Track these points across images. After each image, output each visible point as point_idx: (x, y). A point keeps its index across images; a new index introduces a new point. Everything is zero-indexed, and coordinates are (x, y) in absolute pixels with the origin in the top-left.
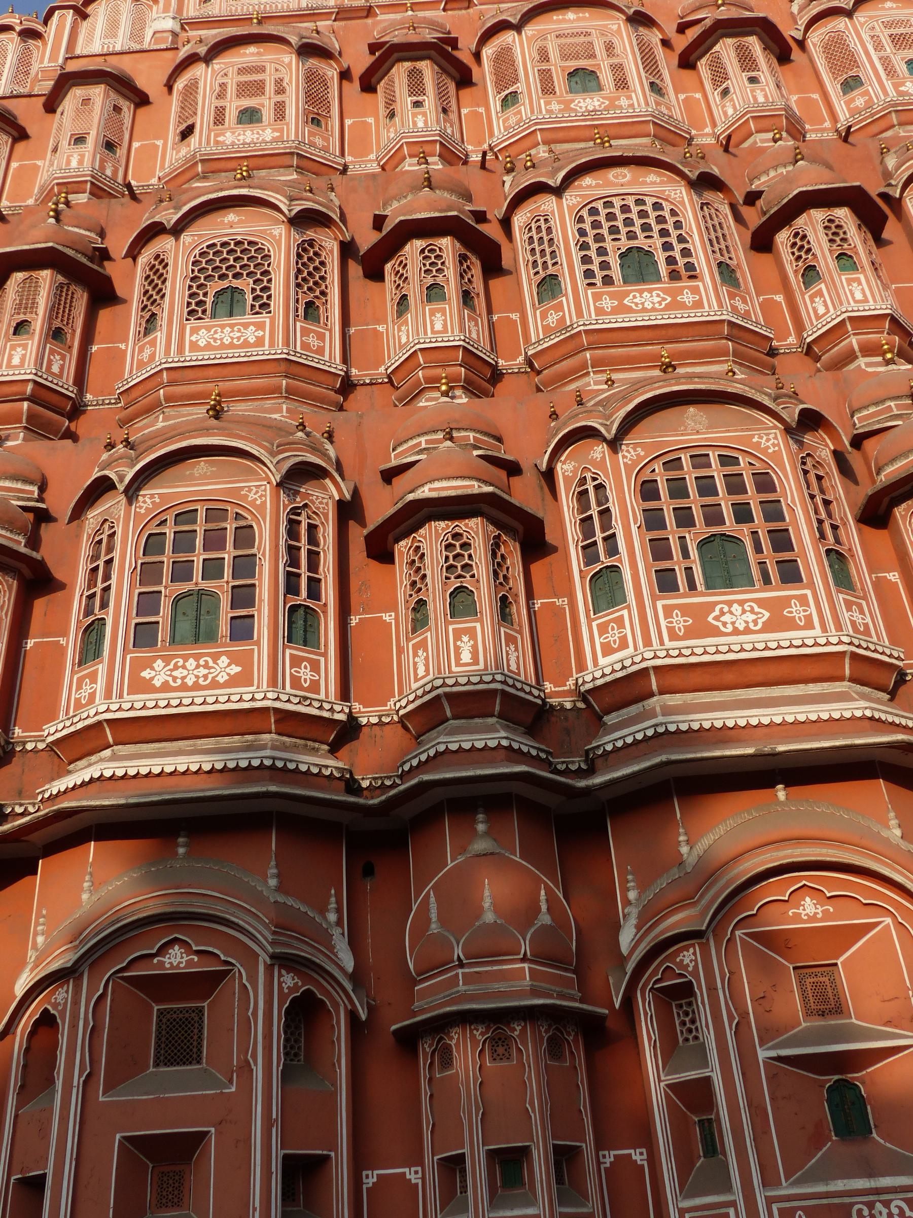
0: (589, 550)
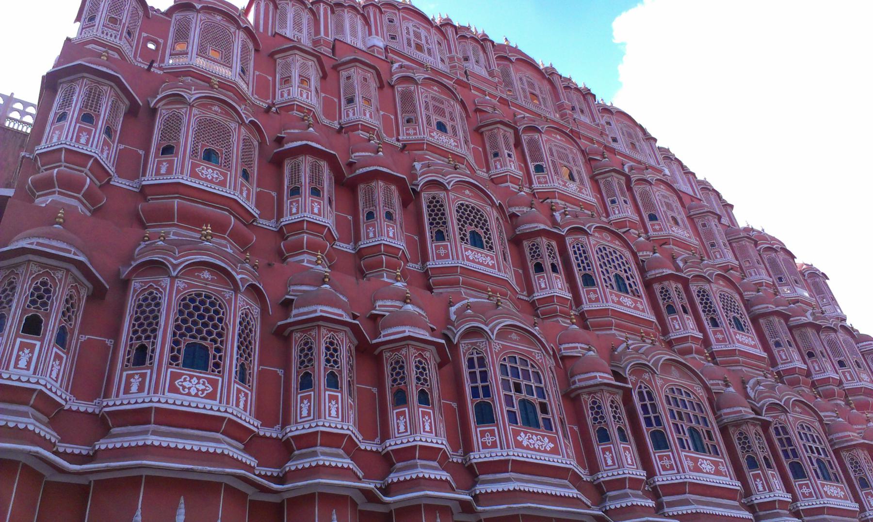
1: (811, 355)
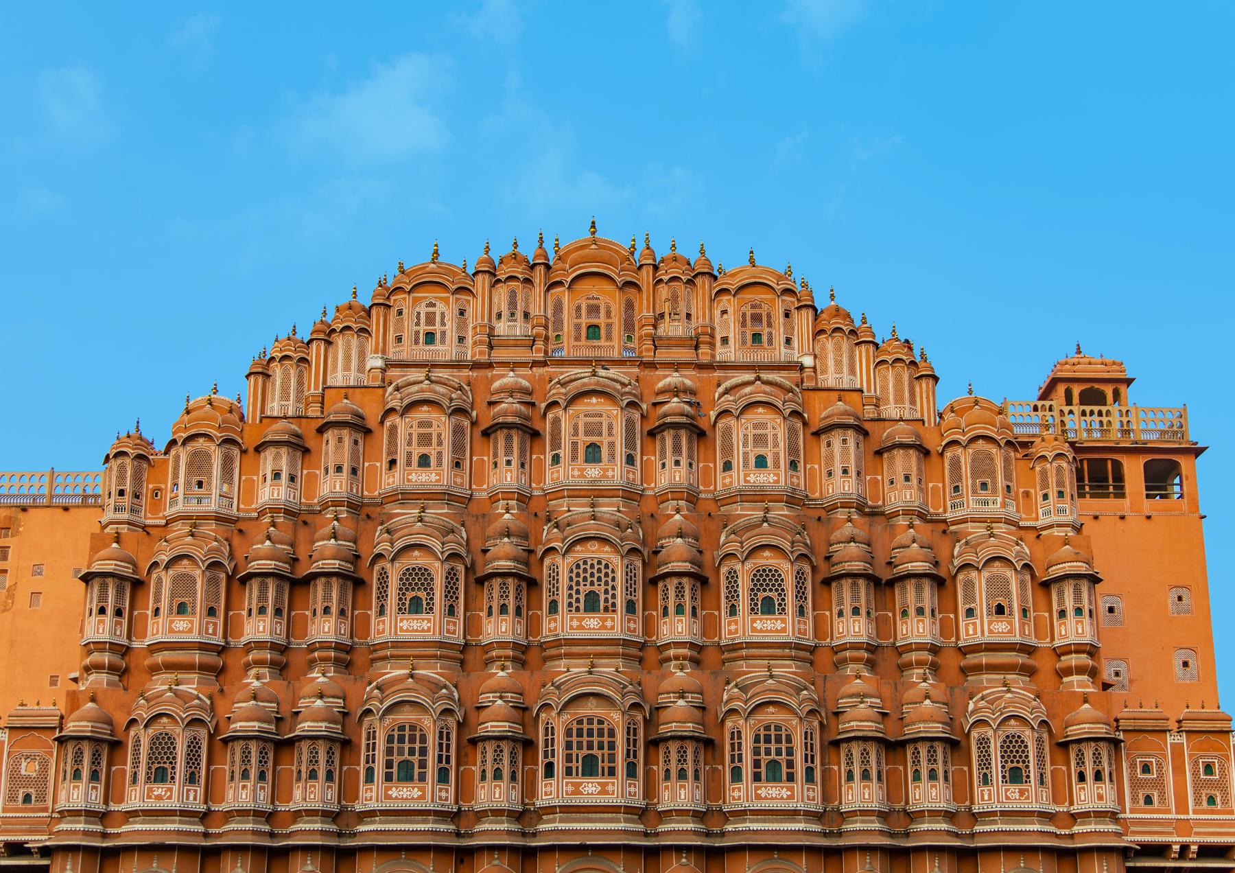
0: (546, 752)
1: (905, 613)
